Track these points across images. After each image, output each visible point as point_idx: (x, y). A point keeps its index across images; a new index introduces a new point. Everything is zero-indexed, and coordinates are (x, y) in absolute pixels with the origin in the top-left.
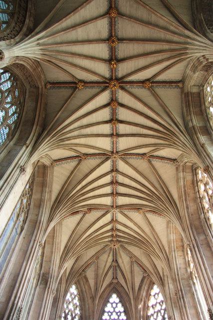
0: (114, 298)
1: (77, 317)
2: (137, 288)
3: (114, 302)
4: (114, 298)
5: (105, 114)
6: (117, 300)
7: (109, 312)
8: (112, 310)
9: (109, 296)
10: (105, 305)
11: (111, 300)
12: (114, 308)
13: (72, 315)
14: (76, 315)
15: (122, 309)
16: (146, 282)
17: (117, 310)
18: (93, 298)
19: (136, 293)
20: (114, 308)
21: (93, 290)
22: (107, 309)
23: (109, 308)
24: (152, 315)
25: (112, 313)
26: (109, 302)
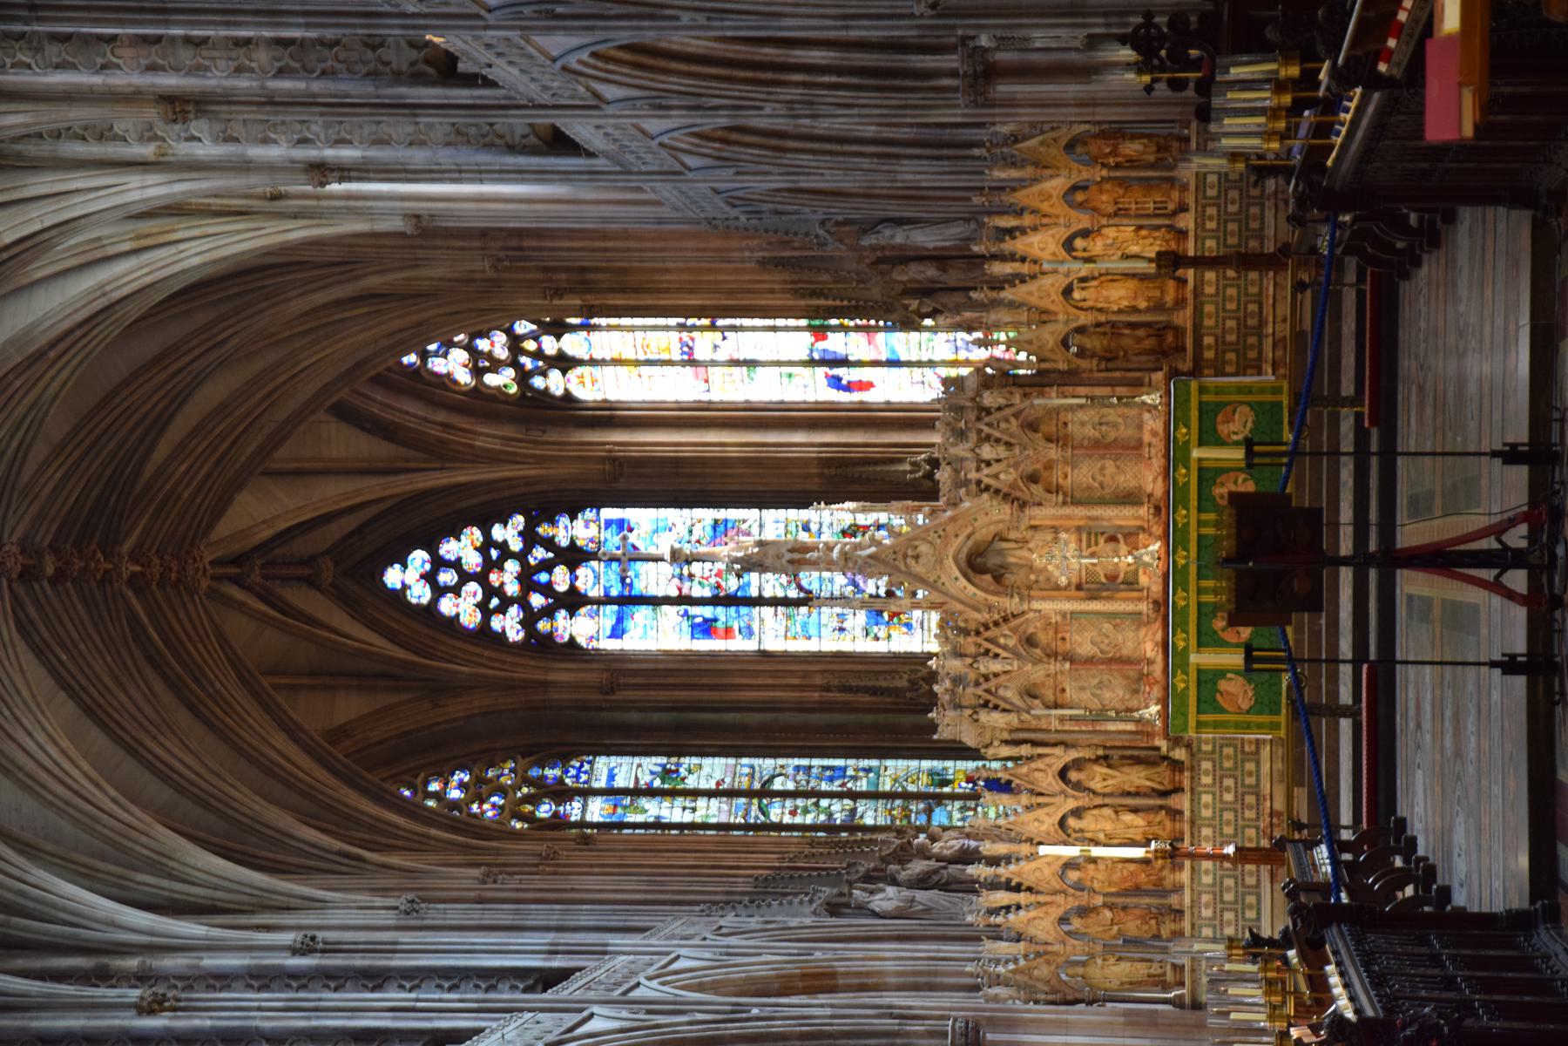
1: (535, 772)
2: (379, 449)
3: (429, 578)
6: (419, 558)
7: (483, 606)
9: (398, 597)
11: (420, 594)
12: (465, 577)
13: (534, 800)
14: (528, 782)
15: (474, 535)
16: (380, 402)
17: (472, 561)
18: (439, 689)
19: (411, 453)
20: (465, 577)
21: (393, 699)
22: (470, 617)
23: (464, 608)
24: (523, 377)
25: (490, 591)
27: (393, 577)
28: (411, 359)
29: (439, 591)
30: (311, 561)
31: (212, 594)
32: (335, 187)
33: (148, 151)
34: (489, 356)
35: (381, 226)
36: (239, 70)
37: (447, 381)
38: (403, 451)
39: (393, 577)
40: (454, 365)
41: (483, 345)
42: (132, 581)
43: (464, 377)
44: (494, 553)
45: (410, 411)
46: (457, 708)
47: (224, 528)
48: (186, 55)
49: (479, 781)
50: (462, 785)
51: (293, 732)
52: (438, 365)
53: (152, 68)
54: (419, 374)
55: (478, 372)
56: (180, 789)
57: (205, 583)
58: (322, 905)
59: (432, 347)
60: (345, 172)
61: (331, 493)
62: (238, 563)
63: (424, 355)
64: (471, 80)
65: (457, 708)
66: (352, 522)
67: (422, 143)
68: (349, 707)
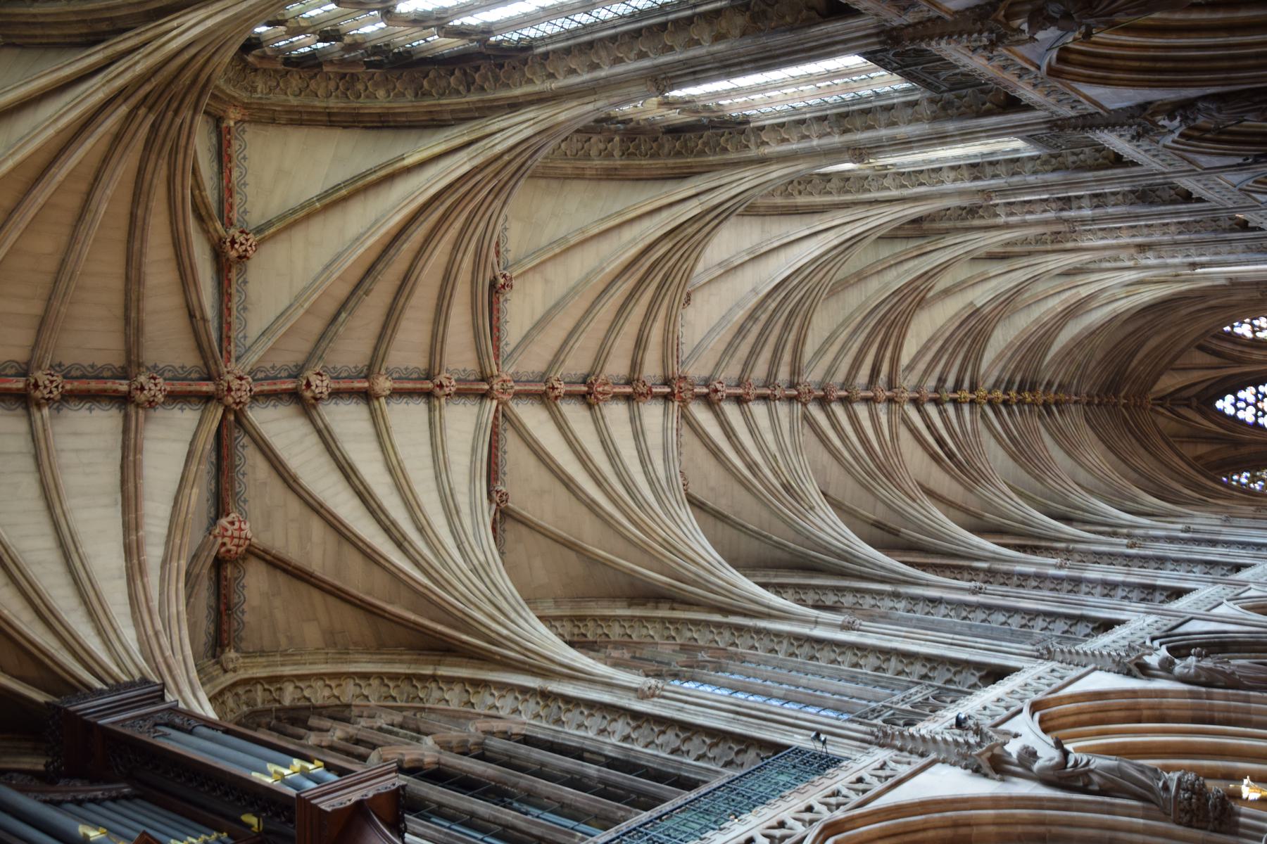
0: (1225, 404)
2: (1215, 360)
3: (1234, 405)
4: (1225, 404)
5: (862, 411)
6: (1230, 398)
7: (1256, 416)
8: (1251, 410)
10: (1243, 422)
11: (1230, 411)
12: (1248, 404)
15: (1252, 390)
16: (1215, 344)
18: (1237, 443)
20: (1248, 404)
21: (1218, 446)
23: (1248, 415)
26: (1234, 417)
27: (1219, 404)
28: (1227, 328)
29: (1237, 409)
30: (1188, 399)
31: (1152, 410)
32: (1199, 271)
33: (1131, 263)
34: (1260, 327)
35: (1216, 283)
36: (1164, 234)
37: (1242, 337)
38: (1223, 361)
39: (1219, 404)
40: (1244, 330)
41: (1256, 322)
42: (1124, 405)
43: (1249, 335)
44: (1260, 396)
45: (1227, 347)
46: (1244, 450)
47: (1157, 388)
48: (1145, 231)
49: (1253, 476)
50: (1246, 478)
51: (1182, 457)
52: (1238, 330)
53: (1134, 236)
54: (1229, 334)
55: (1254, 332)
56: (1140, 474)
57: (1149, 406)
58: (1192, 516)
59: (1236, 324)
60: (1203, 265)
61: (1195, 376)
62: (1161, 400)
63: (1233, 327)
64: (1254, 229)
65: (1244, 450)
66: (1205, 385)
67: (1233, 253)
68: (1202, 449)
